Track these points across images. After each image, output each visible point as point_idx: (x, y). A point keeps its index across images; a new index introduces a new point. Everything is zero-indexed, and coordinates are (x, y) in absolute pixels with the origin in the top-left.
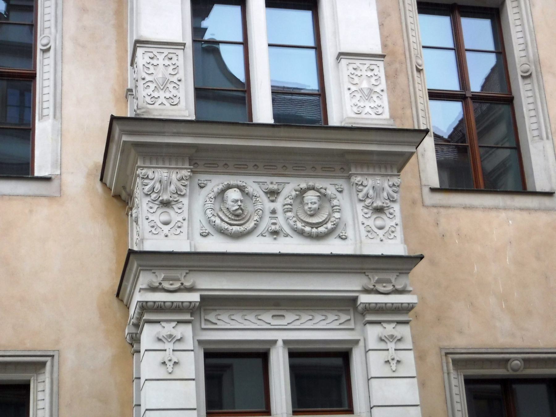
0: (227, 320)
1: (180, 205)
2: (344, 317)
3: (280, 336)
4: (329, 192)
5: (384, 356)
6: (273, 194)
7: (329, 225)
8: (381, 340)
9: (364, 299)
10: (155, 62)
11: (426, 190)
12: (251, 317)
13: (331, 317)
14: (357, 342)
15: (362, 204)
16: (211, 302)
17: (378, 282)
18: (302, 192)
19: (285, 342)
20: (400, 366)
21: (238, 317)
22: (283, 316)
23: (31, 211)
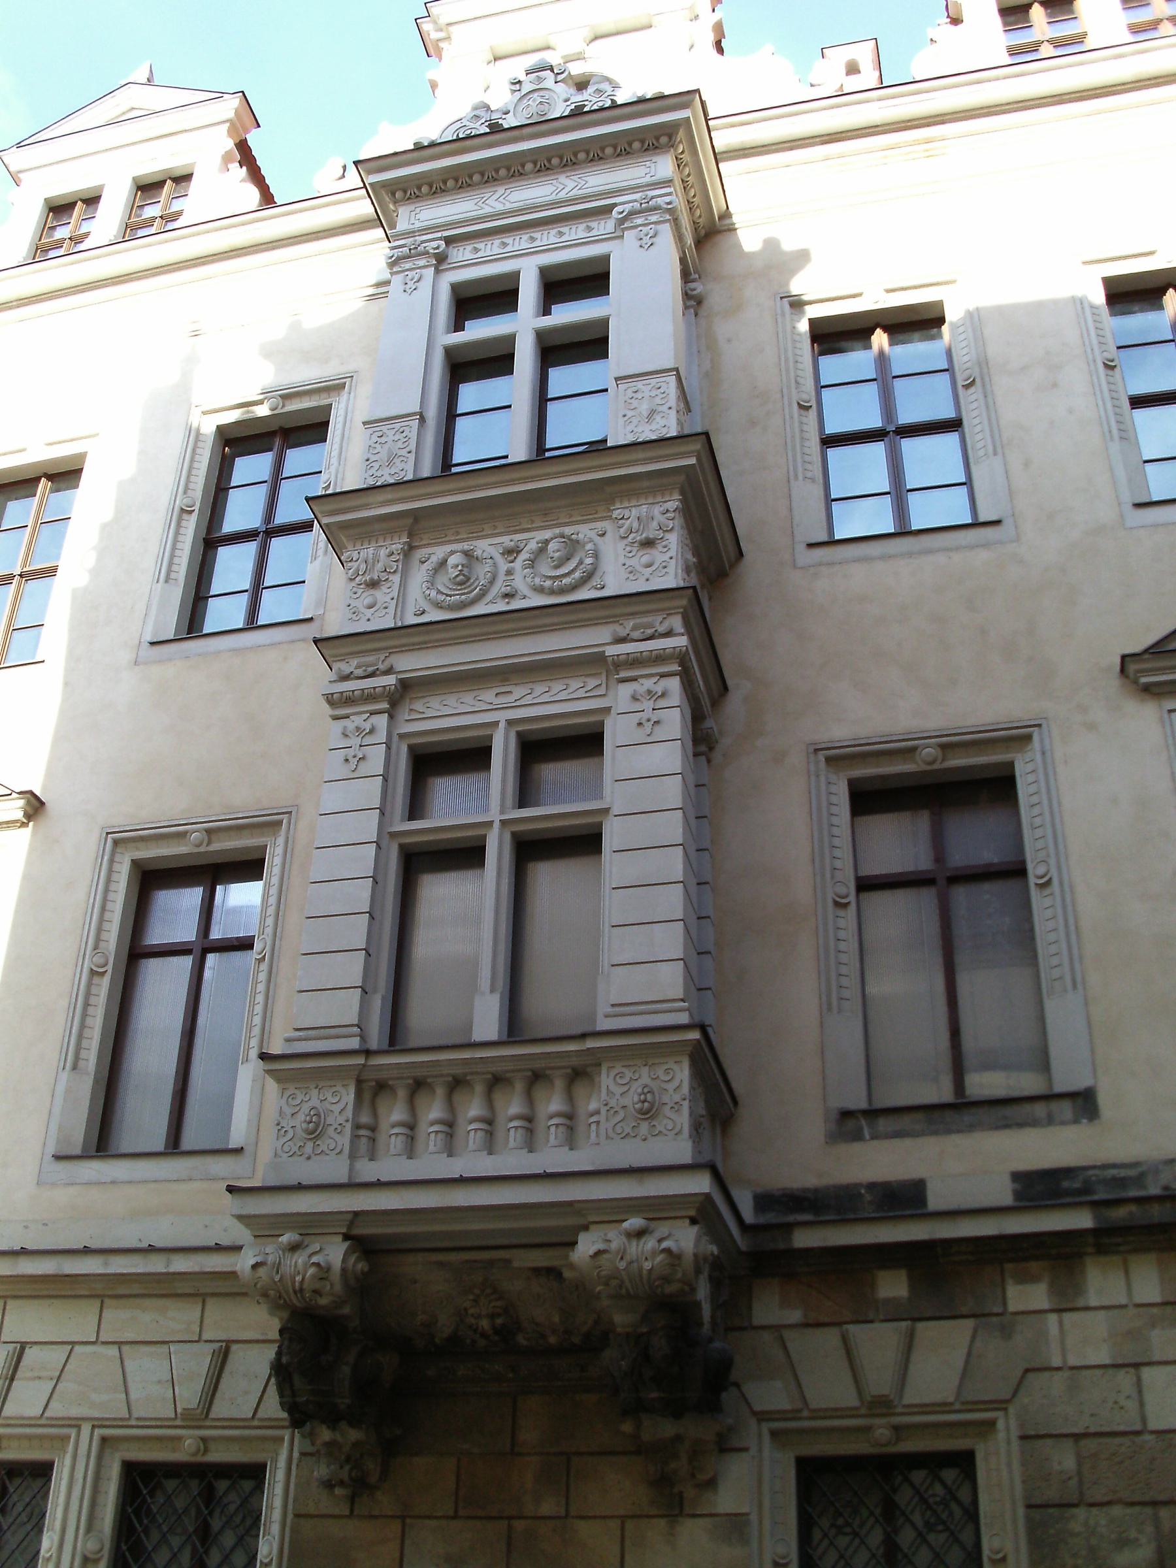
0: (437, 706)
1: (389, 585)
2: (592, 682)
3: (502, 717)
4: (581, 536)
5: (635, 718)
6: (511, 552)
7: (577, 575)
8: (635, 698)
9: (611, 651)
10: (383, 440)
11: (801, 548)
12: (468, 698)
13: (575, 684)
14: (607, 710)
15: (625, 542)
16: (407, 688)
17: (634, 629)
18: (547, 542)
19: (510, 723)
20: (657, 728)
21: (451, 700)
22: (510, 692)
23: (285, 659)
